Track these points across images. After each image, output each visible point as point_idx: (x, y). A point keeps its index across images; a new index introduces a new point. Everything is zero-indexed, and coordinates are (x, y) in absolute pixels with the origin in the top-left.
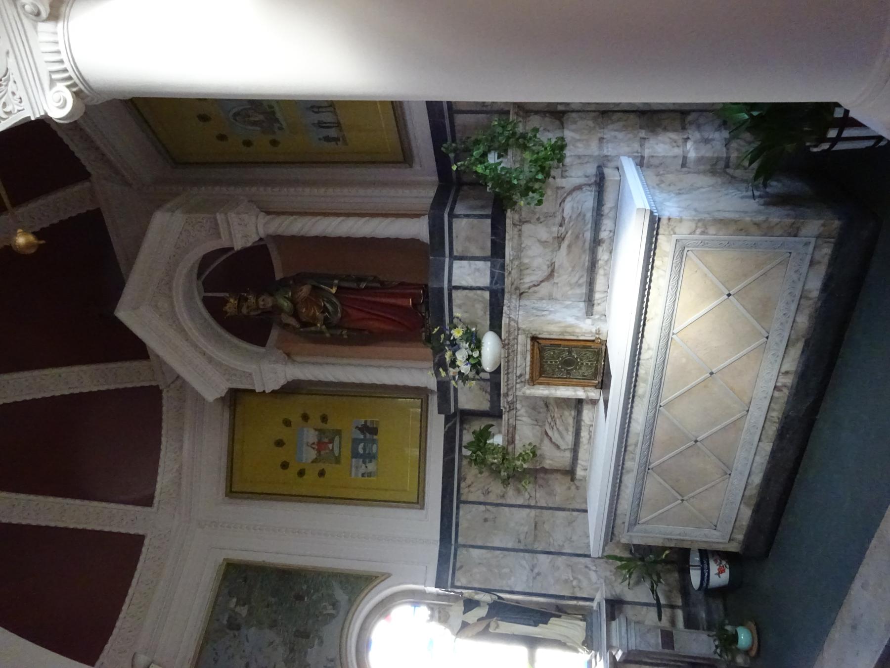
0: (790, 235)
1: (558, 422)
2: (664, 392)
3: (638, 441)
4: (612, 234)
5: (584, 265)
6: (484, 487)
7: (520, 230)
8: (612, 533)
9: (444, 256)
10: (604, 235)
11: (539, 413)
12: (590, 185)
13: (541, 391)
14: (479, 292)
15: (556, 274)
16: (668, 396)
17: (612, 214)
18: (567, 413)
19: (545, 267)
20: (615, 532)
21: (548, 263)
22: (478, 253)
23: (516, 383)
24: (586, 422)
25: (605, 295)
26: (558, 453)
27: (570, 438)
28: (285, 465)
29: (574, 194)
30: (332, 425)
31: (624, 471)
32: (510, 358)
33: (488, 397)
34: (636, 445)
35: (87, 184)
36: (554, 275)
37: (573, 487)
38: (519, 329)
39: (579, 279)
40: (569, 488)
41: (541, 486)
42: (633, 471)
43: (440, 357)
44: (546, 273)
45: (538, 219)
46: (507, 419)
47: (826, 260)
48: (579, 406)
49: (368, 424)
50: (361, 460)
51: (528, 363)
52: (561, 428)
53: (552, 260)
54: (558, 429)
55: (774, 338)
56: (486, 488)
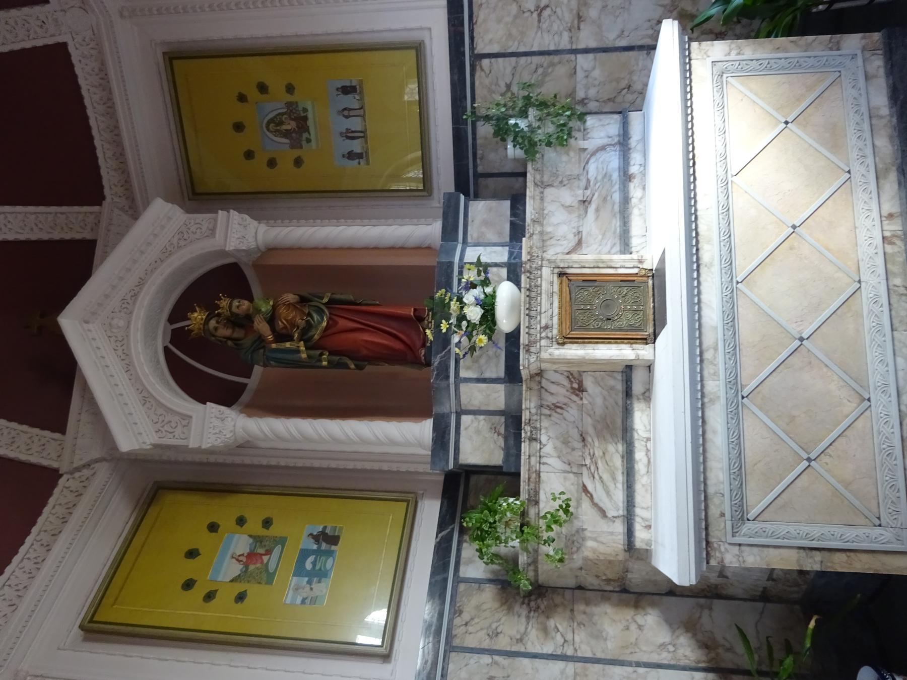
0: (831, 49)
1: (600, 464)
2: (739, 261)
3: (717, 340)
4: (642, 168)
5: (616, 229)
6: (490, 626)
7: (542, 193)
9: (456, 240)
10: (634, 169)
11: (573, 449)
12: (613, 145)
13: (574, 352)
15: (584, 245)
16: (742, 268)
17: (639, 147)
18: (611, 448)
19: (571, 236)
20: (711, 539)
21: (575, 230)
23: (541, 338)
24: (639, 432)
25: (643, 240)
26: (603, 526)
27: (619, 495)
28: (188, 585)
29: (598, 155)
30: (275, 530)
31: (706, 400)
32: (533, 294)
33: (501, 442)
34: (716, 349)
35: (96, 209)
36: (581, 245)
37: (633, 627)
38: (542, 260)
39: (612, 248)
40: (627, 628)
42: (719, 397)
43: (441, 358)
44: (573, 243)
45: (561, 182)
46: (527, 454)
47: (882, 71)
48: (629, 402)
49: (328, 531)
50: (306, 579)
51: (556, 311)
52: (606, 477)
53: (578, 227)
54: (601, 478)
55: (857, 169)
56: (494, 626)
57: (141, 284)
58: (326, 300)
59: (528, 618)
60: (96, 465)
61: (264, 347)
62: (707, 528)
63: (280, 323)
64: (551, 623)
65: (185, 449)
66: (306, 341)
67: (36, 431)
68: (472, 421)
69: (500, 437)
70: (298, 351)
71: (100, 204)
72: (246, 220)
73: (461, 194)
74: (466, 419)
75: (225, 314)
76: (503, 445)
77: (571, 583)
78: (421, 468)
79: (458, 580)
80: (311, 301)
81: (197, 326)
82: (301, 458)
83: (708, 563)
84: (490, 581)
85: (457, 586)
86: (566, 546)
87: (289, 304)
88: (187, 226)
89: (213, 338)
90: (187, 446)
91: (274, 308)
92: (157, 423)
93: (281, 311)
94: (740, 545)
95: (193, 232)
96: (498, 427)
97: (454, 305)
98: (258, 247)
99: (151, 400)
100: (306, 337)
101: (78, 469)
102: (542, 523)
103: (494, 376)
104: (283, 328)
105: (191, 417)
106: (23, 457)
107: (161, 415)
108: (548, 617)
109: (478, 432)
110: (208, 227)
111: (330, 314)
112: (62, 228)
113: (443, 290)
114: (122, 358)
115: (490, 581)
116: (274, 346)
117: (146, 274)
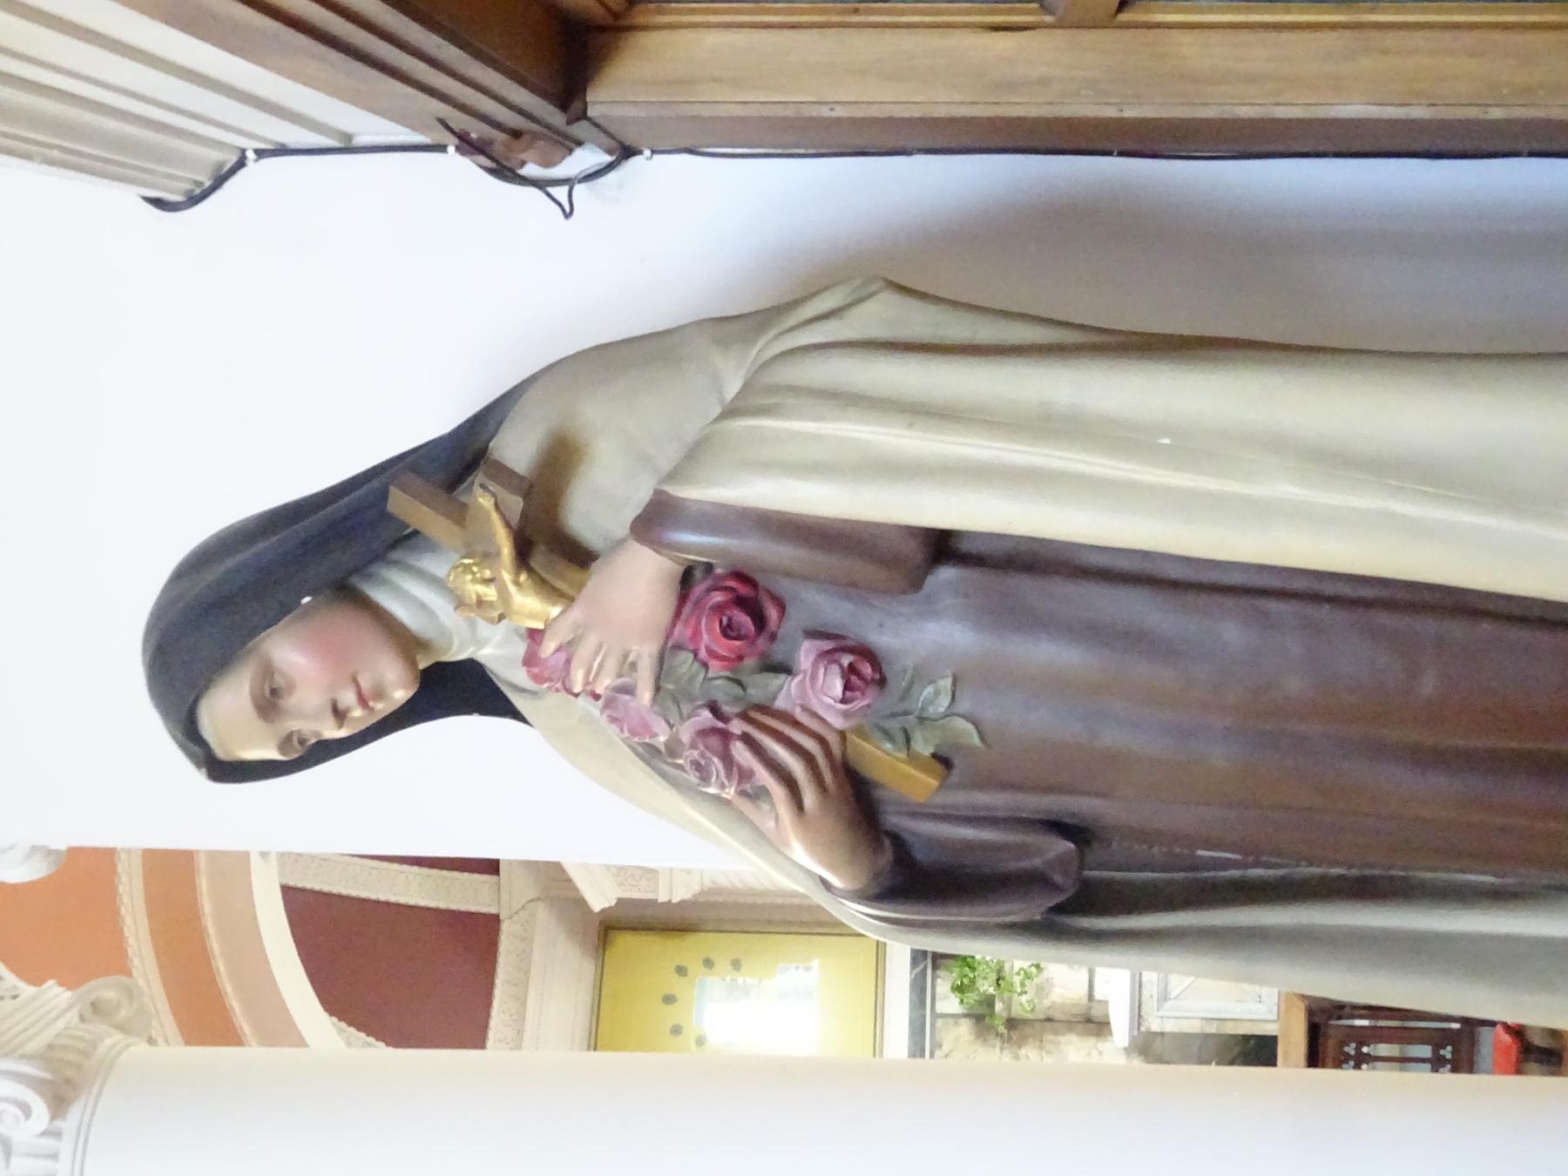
8: (1140, 1016)
20: (1142, 1013)
40: (1089, 1054)
41: (1048, 1052)
59: (1002, 1049)
62: (1140, 1006)
64: (1023, 1052)
65: (652, 903)
77: (1042, 1017)
79: (935, 1016)
83: (1139, 1029)
84: (965, 1016)
85: (935, 1023)
86: (1037, 993)
90: (657, 900)
94: (1162, 1017)
102: (1017, 980)
108: (1020, 1047)
115: (965, 1016)
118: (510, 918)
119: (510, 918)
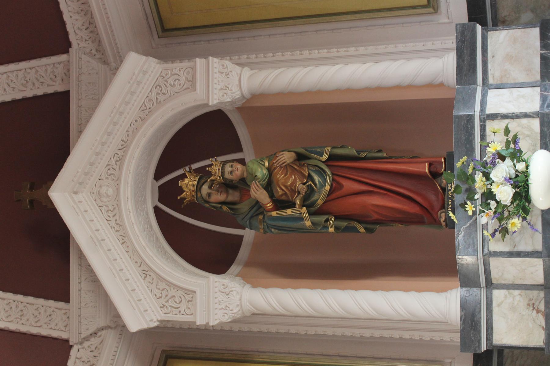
9: (475, 83)
14: (524, 121)
22: (522, 78)
33: (541, 320)
35: (63, 57)
57: (124, 146)
58: (325, 157)
60: (103, 332)
61: (262, 213)
63: (278, 189)
66: (308, 207)
67: (41, 301)
68: (506, 297)
69: (539, 314)
70: (302, 219)
71: (66, 51)
72: (227, 67)
73: (478, 24)
74: (497, 294)
75: (218, 180)
76: (543, 324)
78: (447, 337)
80: (308, 158)
81: (189, 194)
82: (311, 326)
87: (286, 166)
88: (164, 77)
89: (207, 205)
90: (195, 322)
91: (270, 170)
92: (160, 297)
93: (278, 176)
95: (171, 85)
96: (537, 303)
97: (479, 177)
98: (243, 96)
99: (152, 274)
100: (308, 203)
101: (87, 339)
103: (529, 249)
104: (282, 195)
105: (195, 292)
106: (34, 331)
107: (163, 289)
109: (513, 309)
110: (186, 78)
111: (333, 174)
112: (34, 84)
113: (465, 158)
114: (117, 228)
116: (274, 214)
117: (128, 135)
118: (81, 343)
119: (81, 343)
